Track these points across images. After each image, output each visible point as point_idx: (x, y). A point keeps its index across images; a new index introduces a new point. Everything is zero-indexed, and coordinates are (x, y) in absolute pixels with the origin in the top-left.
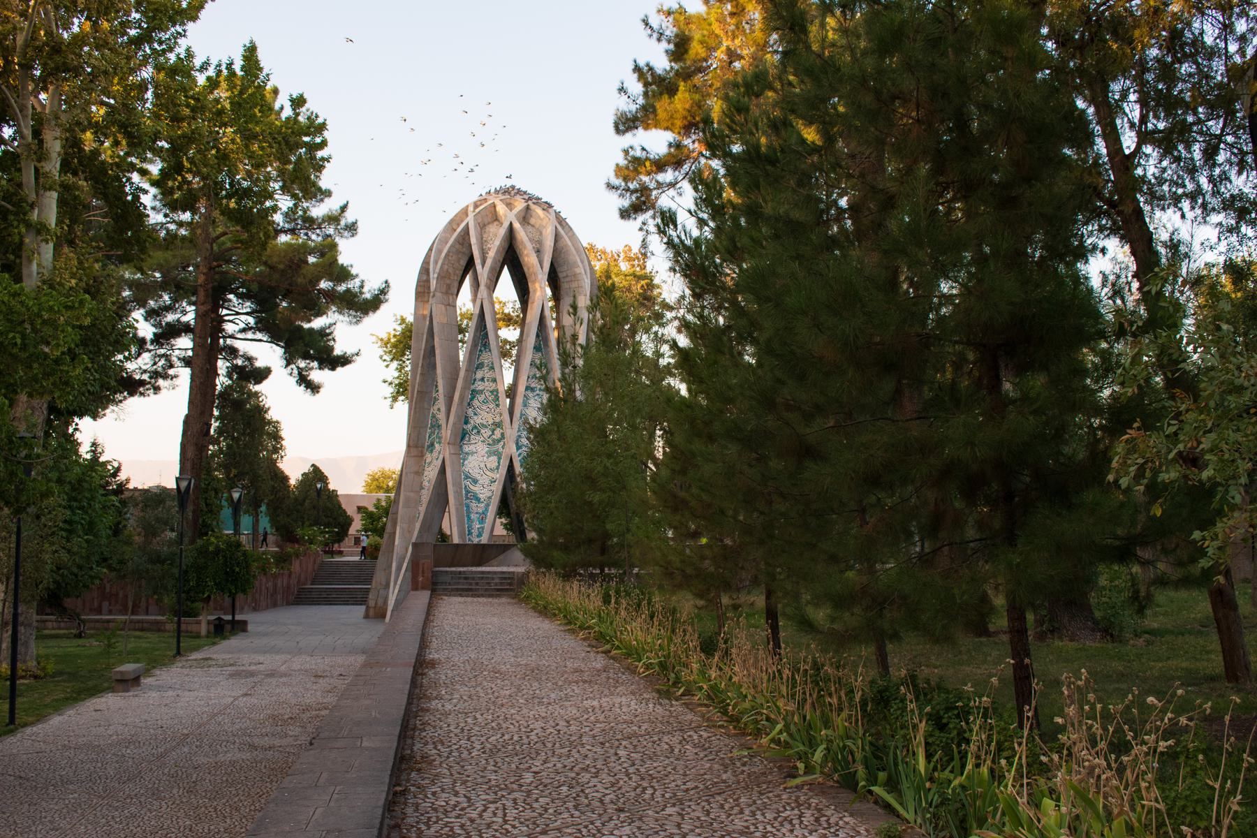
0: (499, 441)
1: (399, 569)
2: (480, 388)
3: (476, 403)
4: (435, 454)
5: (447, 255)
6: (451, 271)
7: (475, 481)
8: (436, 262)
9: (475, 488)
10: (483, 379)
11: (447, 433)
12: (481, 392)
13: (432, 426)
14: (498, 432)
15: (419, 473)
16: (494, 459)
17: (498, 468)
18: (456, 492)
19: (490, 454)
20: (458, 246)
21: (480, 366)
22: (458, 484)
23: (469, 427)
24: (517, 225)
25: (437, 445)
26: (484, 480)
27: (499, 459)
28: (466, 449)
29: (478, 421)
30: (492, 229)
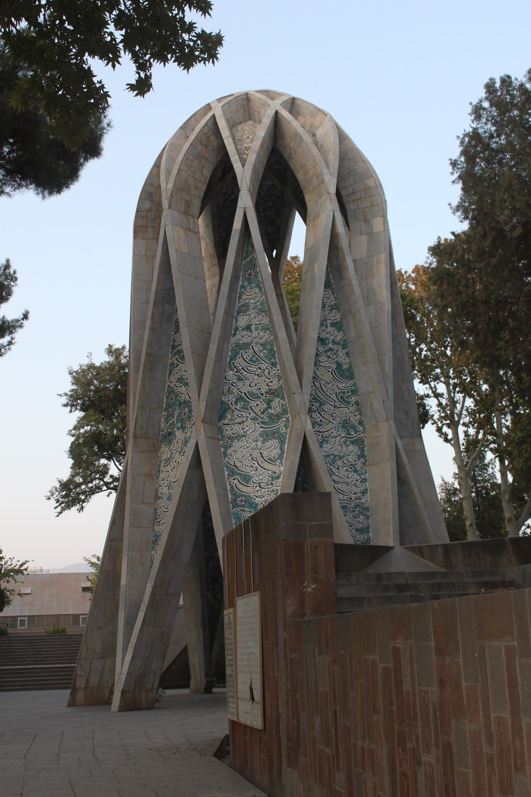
0: (278, 417)
1: (130, 623)
2: (245, 340)
3: (239, 362)
4: (177, 445)
5: (186, 159)
6: (191, 182)
7: (246, 479)
8: (169, 172)
9: (248, 490)
10: (248, 328)
11: (200, 407)
12: (247, 346)
13: (169, 406)
14: (276, 403)
15: (153, 475)
16: (274, 443)
17: (281, 457)
18: (219, 495)
19: (266, 437)
20: (199, 147)
21: (244, 309)
22: (220, 483)
23: (232, 398)
24: (285, 114)
25: (179, 435)
26: (261, 476)
27: (282, 443)
28: (228, 432)
29: (246, 389)
30: (246, 128)
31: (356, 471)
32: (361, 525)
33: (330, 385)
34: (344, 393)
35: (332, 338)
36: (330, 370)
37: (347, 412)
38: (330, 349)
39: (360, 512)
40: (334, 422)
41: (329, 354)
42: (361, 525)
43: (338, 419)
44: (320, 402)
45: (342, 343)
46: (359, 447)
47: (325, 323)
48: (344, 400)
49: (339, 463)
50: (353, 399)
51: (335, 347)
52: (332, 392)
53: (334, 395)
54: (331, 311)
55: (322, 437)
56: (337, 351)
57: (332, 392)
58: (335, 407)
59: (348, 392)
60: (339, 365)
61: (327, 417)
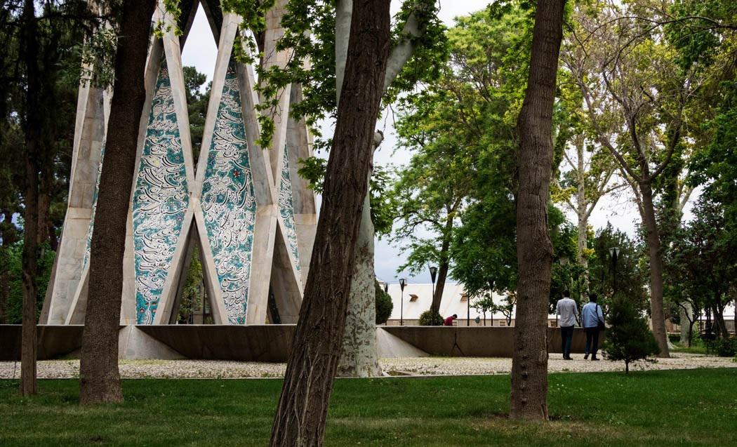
31: (167, 241)
32: (157, 287)
33: (160, 170)
34: (172, 175)
35: (166, 129)
36: (162, 157)
37: (171, 191)
38: (163, 139)
39: (160, 276)
40: (160, 201)
41: (161, 143)
42: (157, 287)
43: (164, 198)
44: (149, 185)
45: (176, 132)
46: (177, 221)
47: (161, 117)
48: (171, 181)
49: (154, 235)
50: (181, 180)
51: (168, 137)
52: (161, 176)
53: (163, 178)
54: (169, 105)
55: (145, 215)
56: (170, 140)
57: (161, 176)
58: (162, 188)
59: (177, 174)
60: (171, 152)
61: (154, 197)
